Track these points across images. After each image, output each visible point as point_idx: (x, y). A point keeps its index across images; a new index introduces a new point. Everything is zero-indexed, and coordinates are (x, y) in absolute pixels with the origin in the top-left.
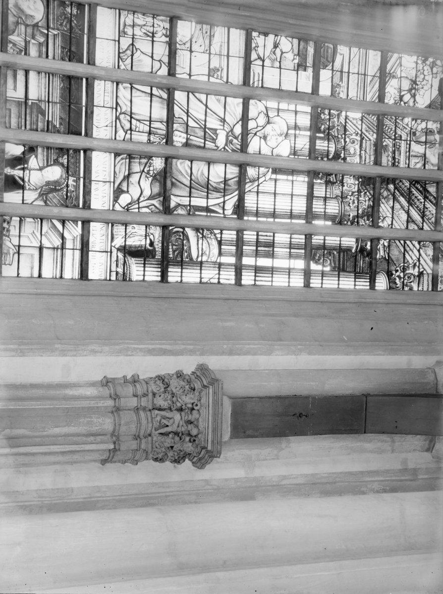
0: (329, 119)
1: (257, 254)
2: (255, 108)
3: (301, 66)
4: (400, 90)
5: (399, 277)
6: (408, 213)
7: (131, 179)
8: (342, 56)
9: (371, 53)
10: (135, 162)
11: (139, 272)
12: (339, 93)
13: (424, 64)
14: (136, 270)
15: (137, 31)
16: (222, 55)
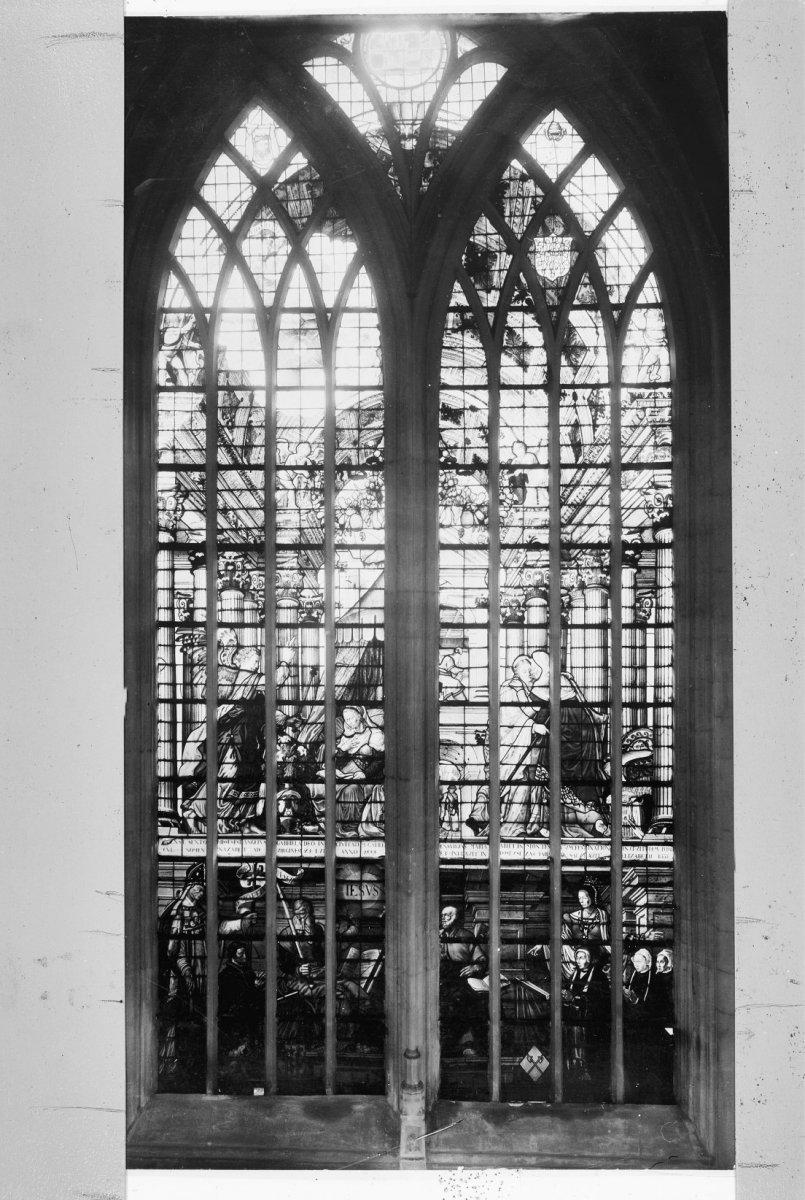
0: (511, 607)
1: (644, 687)
2: (507, 695)
4: (474, 525)
5: (659, 513)
6: (593, 506)
15: (455, 818)
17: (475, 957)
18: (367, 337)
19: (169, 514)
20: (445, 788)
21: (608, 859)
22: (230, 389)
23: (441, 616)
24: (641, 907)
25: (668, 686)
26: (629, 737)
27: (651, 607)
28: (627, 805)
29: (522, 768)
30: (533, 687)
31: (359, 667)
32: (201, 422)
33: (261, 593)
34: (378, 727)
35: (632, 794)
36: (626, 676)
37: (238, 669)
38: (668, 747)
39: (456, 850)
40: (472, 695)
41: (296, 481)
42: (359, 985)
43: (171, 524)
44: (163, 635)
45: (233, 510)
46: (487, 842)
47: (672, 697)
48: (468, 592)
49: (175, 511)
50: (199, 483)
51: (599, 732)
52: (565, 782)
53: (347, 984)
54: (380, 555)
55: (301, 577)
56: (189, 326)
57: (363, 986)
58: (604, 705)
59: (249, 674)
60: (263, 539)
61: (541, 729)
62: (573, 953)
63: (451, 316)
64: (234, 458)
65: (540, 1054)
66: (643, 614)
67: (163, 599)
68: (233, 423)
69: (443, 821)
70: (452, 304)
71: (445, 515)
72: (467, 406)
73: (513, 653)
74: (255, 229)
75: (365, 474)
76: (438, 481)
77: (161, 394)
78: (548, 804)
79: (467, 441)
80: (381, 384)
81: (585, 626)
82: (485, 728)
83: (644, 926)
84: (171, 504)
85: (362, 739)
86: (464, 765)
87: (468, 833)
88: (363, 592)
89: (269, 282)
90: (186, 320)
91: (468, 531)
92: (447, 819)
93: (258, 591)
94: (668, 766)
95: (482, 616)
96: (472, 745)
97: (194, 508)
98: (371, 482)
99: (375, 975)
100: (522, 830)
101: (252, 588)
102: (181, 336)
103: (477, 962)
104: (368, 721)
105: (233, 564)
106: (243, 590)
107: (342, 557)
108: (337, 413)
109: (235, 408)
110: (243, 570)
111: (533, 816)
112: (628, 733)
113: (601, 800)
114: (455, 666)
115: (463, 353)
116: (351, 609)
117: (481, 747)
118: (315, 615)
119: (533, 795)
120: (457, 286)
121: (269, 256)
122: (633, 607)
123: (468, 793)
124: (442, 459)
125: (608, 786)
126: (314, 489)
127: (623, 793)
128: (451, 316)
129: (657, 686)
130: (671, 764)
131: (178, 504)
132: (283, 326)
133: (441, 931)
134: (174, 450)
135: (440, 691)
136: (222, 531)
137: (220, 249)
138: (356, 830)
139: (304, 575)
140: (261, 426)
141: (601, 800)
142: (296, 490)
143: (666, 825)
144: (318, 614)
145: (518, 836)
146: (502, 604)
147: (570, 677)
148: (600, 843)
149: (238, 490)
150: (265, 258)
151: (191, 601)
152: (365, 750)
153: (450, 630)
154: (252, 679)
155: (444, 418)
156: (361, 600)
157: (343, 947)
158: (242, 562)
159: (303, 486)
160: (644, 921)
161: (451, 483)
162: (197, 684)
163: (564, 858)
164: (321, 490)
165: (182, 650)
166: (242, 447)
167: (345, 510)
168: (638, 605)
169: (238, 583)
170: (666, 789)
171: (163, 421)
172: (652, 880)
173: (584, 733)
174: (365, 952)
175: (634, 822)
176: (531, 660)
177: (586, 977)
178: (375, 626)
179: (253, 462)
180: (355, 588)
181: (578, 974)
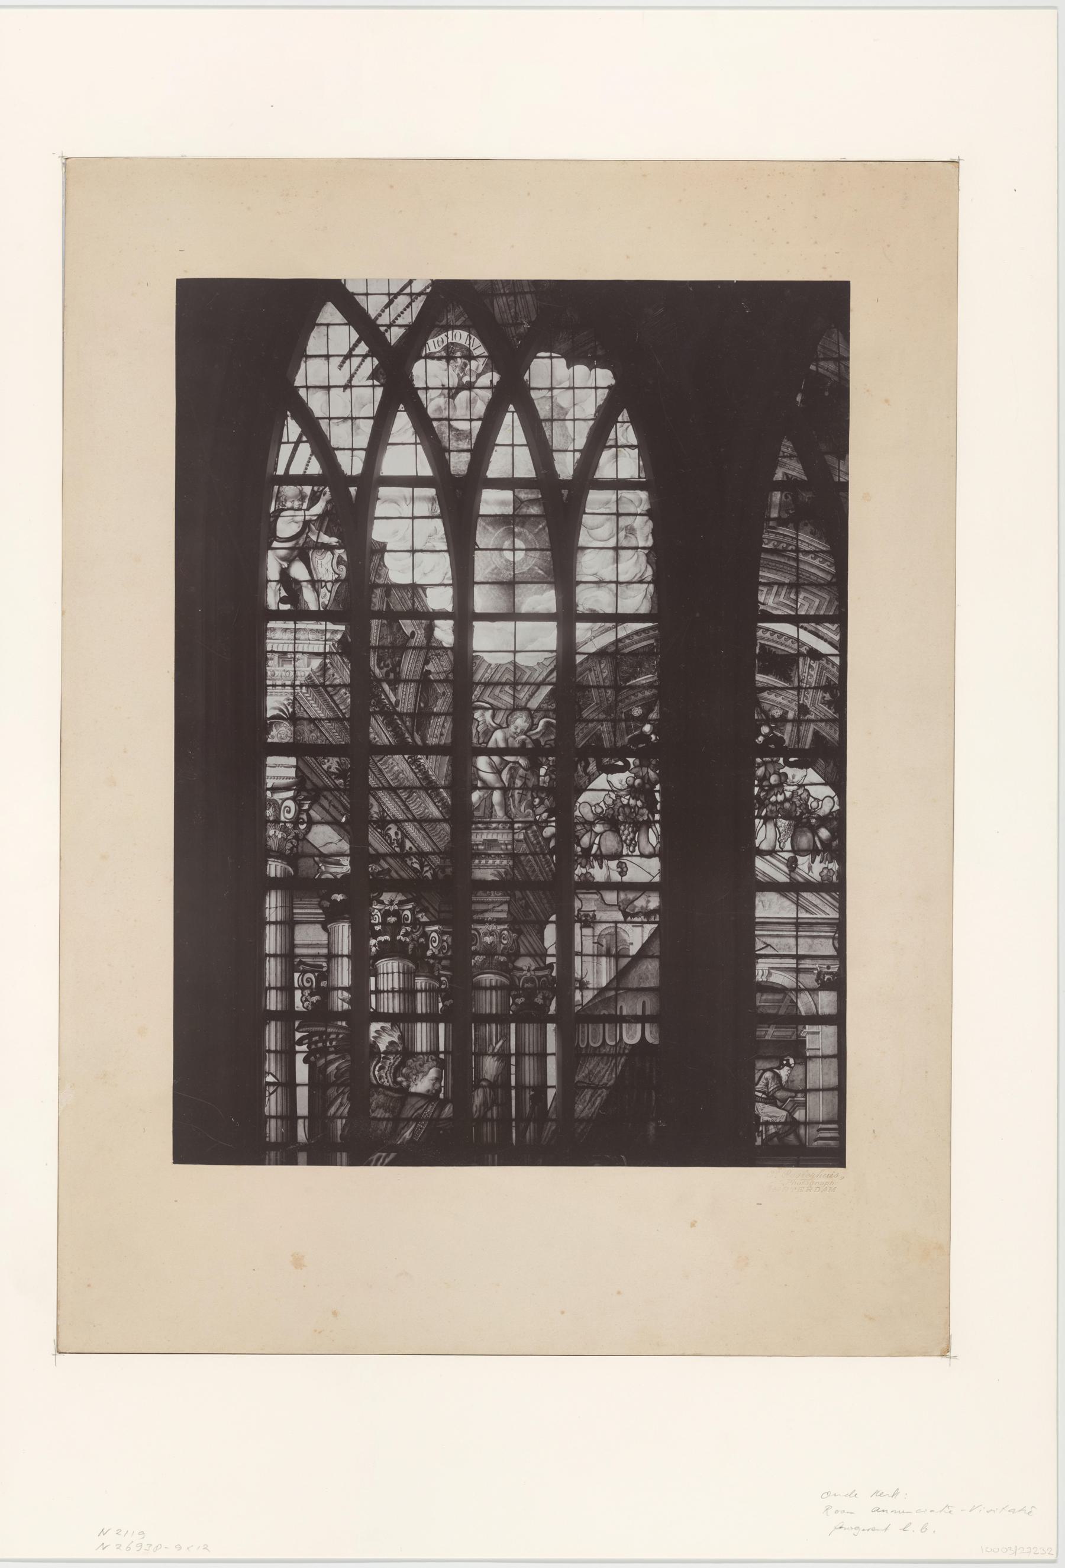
3: (797, 1051)
4: (813, 852)
8: (772, 971)
9: (760, 913)
12: (831, 973)
13: (767, 802)
18: (631, 531)
19: (284, 829)
22: (392, 617)
32: (342, 674)
33: (444, 962)
37: (405, 1093)
41: (505, 775)
43: (289, 845)
44: (272, 1035)
45: (396, 822)
48: (807, 964)
49: (296, 821)
50: (338, 777)
54: (654, 902)
55: (514, 935)
56: (318, 508)
59: (422, 1103)
60: (449, 871)
63: (777, 497)
64: (397, 733)
67: (273, 971)
68: (398, 674)
70: (779, 476)
71: (765, 835)
72: (804, 650)
74: (434, 345)
75: (627, 764)
76: (753, 776)
77: (271, 624)
79: (803, 709)
80: (655, 611)
84: (289, 810)
88: (624, 962)
89: (460, 434)
90: (314, 499)
91: (803, 861)
93: (441, 959)
97: (329, 818)
98: (636, 777)
101: (429, 953)
102: (306, 524)
105: (396, 913)
106: (412, 958)
107: (587, 903)
108: (579, 659)
109: (400, 646)
110: (415, 922)
114: (781, 1087)
115: (797, 560)
116: (602, 991)
118: (539, 1000)
120: (787, 447)
121: (460, 388)
124: (761, 739)
126: (537, 789)
128: (777, 497)
131: (299, 811)
132: (484, 509)
134: (293, 719)
136: (378, 857)
137: (373, 376)
139: (520, 933)
140: (446, 680)
142: (505, 790)
144: (544, 998)
149: (405, 788)
150: (452, 393)
151: (324, 975)
154: (430, 1109)
155: (765, 671)
156: (621, 975)
158: (412, 910)
159: (519, 783)
161: (773, 779)
162: (334, 1117)
164: (549, 790)
165: (305, 1061)
166: (410, 715)
167: (592, 824)
169: (406, 944)
171: (276, 669)
179: (432, 741)
180: (608, 954)
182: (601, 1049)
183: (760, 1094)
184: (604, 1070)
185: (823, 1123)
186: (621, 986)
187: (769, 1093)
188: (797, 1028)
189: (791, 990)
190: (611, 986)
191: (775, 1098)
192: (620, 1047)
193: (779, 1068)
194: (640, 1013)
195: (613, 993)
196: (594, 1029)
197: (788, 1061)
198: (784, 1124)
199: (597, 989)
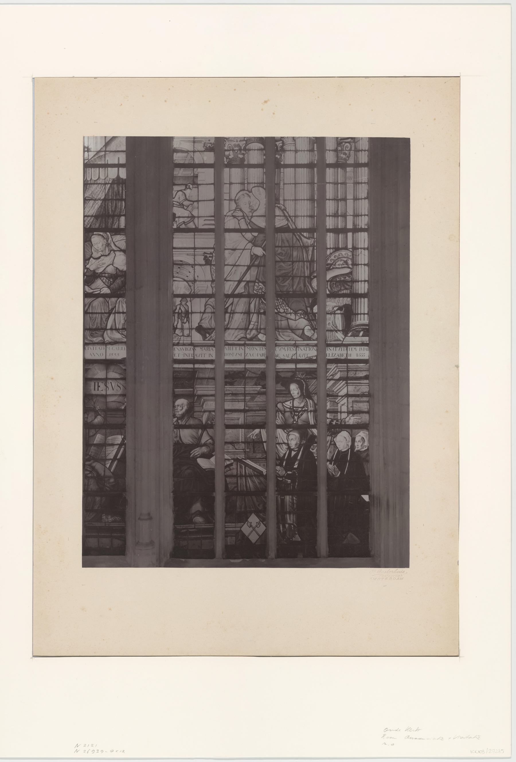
0: (233, 150)
1: (345, 216)
2: (230, 223)
3: (194, 181)
7: (294, 327)
10: (281, 324)
11: (362, 318)
12: (211, 143)
14: (363, 320)
16: (194, 254)
17: (203, 441)
20: (178, 300)
21: (315, 358)
23: (175, 158)
24: (342, 396)
25: (365, 215)
26: (332, 257)
27: (350, 150)
28: (331, 314)
29: (243, 284)
30: (252, 217)
31: (105, 200)
34: (121, 250)
35: (334, 304)
36: (330, 207)
38: (365, 265)
39: (187, 352)
40: (201, 224)
42: (105, 465)
46: (213, 346)
47: (368, 225)
51: (307, 252)
52: (279, 295)
53: (94, 464)
57: (108, 466)
58: (311, 231)
61: (259, 251)
62: (285, 435)
65: (258, 520)
66: (344, 156)
69: (176, 328)
73: (236, 188)
78: (264, 313)
81: (296, 166)
82: (212, 251)
83: (344, 412)
85: (107, 260)
86: (195, 281)
87: (197, 337)
92: (179, 326)
94: (365, 281)
95: (209, 158)
96: (201, 265)
99: (118, 457)
100: (242, 335)
103: (205, 445)
104: (112, 245)
111: (252, 323)
112: (331, 254)
113: (309, 309)
114: (186, 199)
116: (98, 152)
117: (208, 267)
119: (252, 306)
122: (336, 150)
123: (198, 305)
125: (314, 298)
127: (328, 304)
129: (356, 215)
130: (367, 279)
133: (175, 419)
135: (174, 220)
138: (102, 336)
141: (309, 309)
143: (363, 330)
145: (239, 340)
146: (226, 148)
147: (283, 207)
148: (308, 345)
152: (110, 270)
153: (182, 169)
157: (91, 434)
160: (344, 409)
163: (278, 358)
168: (340, 148)
170: (362, 299)
172: (351, 374)
173: (295, 254)
174: (110, 438)
175: (336, 327)
176: (250, 194)
177: (297, 455)
178: (119, 166)
181: (290, 453)
182: (98, 181)
183: (176, 203)
184: (99, 191)
185: (206, 217)
186: (107, 150)
187: (180, 202)
188: (193, 170)
189: (191, 151)
190: (102, 150)
191: (183, 205)
192: (107, 180)
193: (185, 190)
194: (117, 163)
195: (103, 153)
196: (94, 171)
197: (189, 186)
198: (188, 217)
199: (96, 151)
